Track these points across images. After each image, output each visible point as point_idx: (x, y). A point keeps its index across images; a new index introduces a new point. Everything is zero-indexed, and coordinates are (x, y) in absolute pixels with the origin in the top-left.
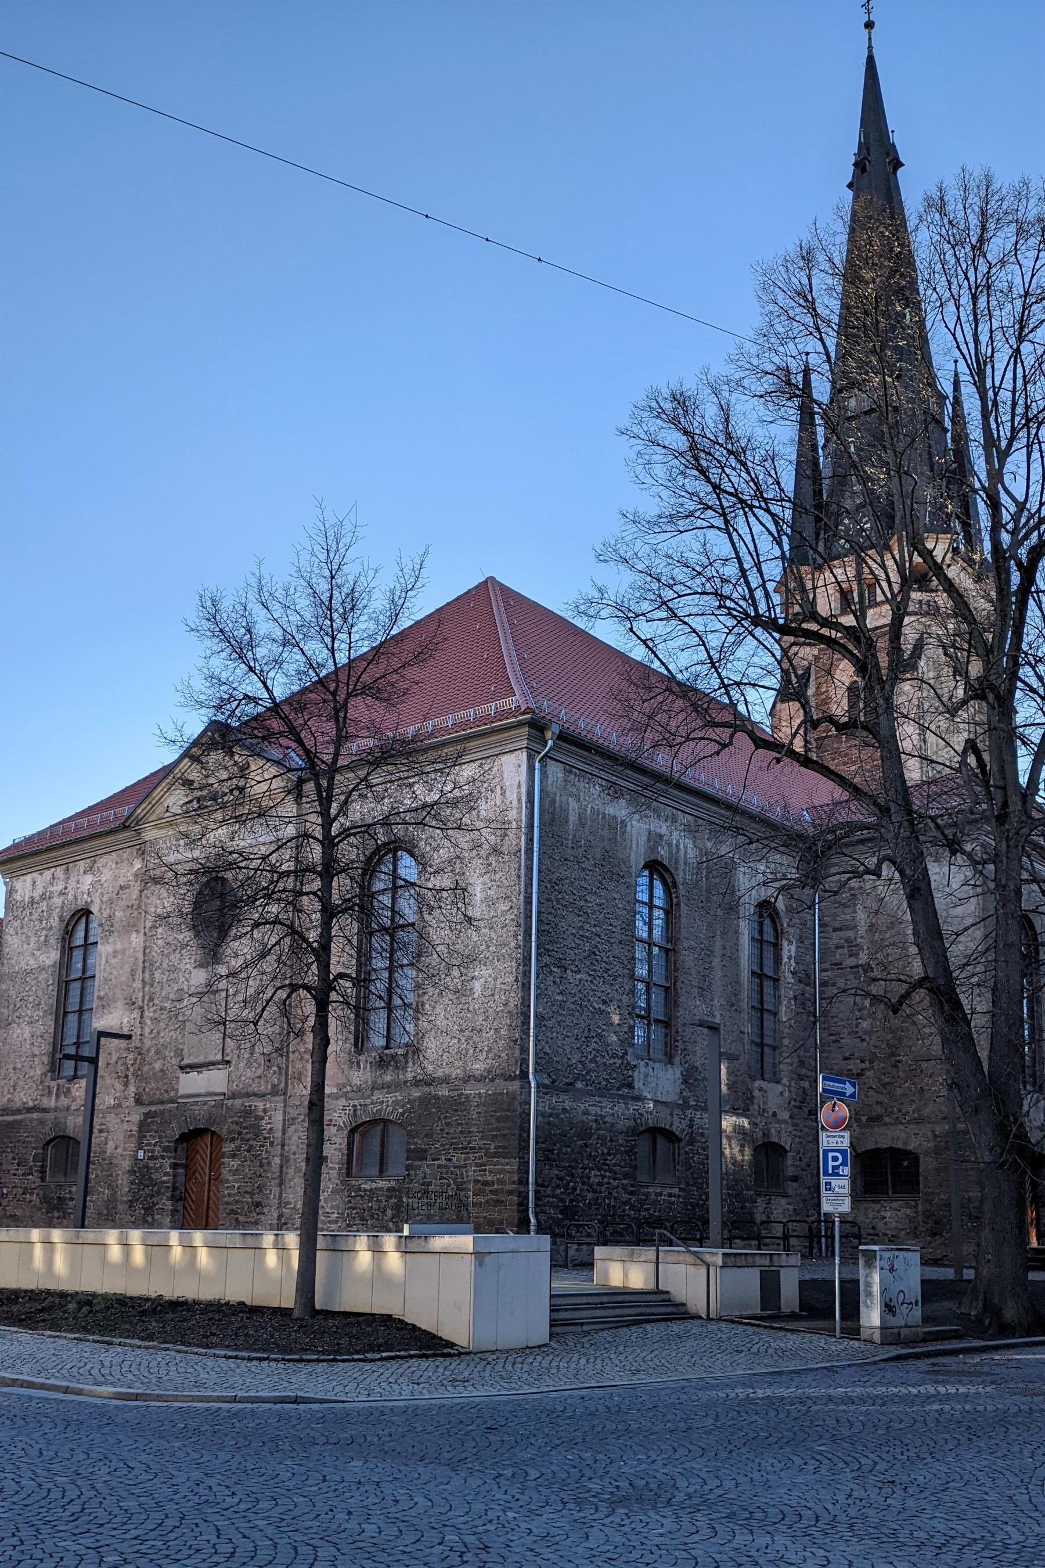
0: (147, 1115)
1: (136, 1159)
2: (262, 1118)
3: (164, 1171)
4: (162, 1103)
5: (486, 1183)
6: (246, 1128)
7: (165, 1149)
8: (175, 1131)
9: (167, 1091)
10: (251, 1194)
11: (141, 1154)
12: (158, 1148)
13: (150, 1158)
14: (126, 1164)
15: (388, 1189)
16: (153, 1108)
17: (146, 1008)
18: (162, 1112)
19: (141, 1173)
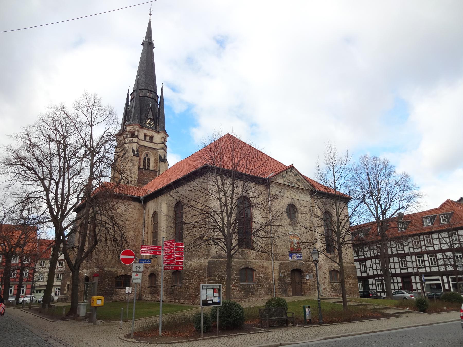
0: (281, 264)
1: (279, 276)
2: (313, 268)
3: (288, 279)
4: (284, 261)
5: (354, 283)
6: (309, 269)
7: (288, 274)
8: (290, 269)
10: (313, 286)
11: (281, 275)
12: (285, 273)
13: (283, 276)
14: (277, 278)
15: (338, 285)
16: (283, 262)
18: (286, 263)
19: (281, 280)
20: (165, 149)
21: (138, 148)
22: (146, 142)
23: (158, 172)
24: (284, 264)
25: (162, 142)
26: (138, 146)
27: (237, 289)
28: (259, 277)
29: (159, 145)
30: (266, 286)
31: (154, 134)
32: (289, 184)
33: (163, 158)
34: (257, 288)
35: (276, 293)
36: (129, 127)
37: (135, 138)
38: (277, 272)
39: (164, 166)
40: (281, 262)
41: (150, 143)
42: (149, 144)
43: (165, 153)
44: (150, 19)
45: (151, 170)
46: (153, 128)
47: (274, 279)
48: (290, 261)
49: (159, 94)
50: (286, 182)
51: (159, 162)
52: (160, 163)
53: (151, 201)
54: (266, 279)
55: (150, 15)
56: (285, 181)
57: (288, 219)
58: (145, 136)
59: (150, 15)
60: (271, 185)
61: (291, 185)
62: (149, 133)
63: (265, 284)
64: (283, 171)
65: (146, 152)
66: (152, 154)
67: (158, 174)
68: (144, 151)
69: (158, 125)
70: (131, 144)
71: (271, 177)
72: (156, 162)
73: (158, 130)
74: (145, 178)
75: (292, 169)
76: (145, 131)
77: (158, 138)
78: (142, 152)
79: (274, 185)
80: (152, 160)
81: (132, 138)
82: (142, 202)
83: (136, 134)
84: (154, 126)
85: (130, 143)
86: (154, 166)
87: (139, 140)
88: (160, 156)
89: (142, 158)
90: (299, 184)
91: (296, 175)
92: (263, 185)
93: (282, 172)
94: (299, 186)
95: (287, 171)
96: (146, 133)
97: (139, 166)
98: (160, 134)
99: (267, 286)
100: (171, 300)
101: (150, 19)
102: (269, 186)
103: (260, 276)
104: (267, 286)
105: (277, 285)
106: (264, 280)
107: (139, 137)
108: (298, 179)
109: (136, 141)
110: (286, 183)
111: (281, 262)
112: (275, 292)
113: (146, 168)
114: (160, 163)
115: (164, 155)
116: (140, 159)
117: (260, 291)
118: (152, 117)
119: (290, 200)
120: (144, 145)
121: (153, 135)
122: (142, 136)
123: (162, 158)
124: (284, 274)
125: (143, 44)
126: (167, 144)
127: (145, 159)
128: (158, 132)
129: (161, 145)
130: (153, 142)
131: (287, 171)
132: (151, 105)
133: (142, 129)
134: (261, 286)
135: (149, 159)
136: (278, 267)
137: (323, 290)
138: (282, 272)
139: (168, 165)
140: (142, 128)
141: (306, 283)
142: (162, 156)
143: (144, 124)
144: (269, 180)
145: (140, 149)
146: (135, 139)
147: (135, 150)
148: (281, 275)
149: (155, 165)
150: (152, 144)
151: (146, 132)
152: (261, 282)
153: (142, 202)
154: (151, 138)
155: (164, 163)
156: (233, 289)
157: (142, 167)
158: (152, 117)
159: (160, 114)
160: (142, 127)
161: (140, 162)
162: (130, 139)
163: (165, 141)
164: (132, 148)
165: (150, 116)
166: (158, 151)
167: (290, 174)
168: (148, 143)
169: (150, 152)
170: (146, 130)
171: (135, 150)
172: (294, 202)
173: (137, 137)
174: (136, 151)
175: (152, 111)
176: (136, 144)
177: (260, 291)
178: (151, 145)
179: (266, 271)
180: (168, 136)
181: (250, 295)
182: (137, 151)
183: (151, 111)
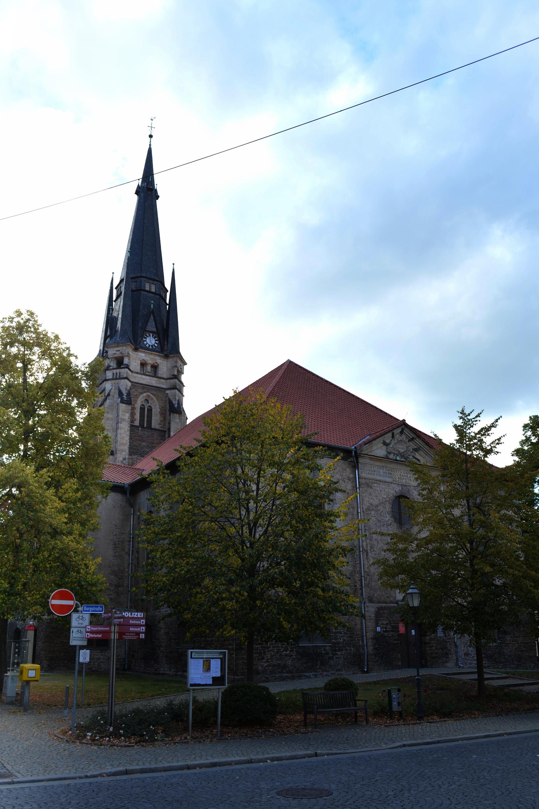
0: (379, 609)
4: (386, 603)
9: (388, 597)
11: (379, 629)
12: (389, 626)
13: (384, 631)
14: (370, 635)
16: (384, 605)
17: (369, 551)
20: (178, 387)
21: (128, 388)
22: (144, 377)
23: (167, 433)
24: (385, 608)
25: (174, 375)
26: (129, 384)
27: (291, 656)
28: (336, 633)
29: (168, 381)
30: (351, 650)
31: (159, 360)
32: (398, 458)
33: (176, 406)
34: (332, 654)
35: (369, 663)
36: (112, 349)
37: (123, 370)
38: (371, 624)
39: (178, 420)
40: (380, 605)
41: (151, 378)
42: (149, 380)
43: (179, 397)
44: (150, 145)
45: (155, 429)
46: (157, 349)
47: (365, 637)
48: (397, 603)
49: (168, 285)
50: (392, 455)
51: (168, 413)
52: (171, 416)
53: (143, 492)
54: (350, 637)
55: (151, 136)
56: (389, 453)
57: (395, 525)
58: (143, 365)
59: (151, 136)
60: (361, 460)
61: (402, 459)
62: (150, 358)
63: (348, 646)
64: (386, 433)
65: (145, 394)
66: (155, 399)
67: (167, 436)
68: (140, 393)
69: (166, 343)
70: (117, 381)
71: (360, 445)
72: (163, 413)
73: (165, 353)
74: (144, 444)
75: (403, 429)
76: (142, 355)
77: (164, 367)
78: (137, 396)
79: (367, 461)
80: (156, 410)
81: (118, 371)
82: (128, 492)
83: (126, 361)
84: (159, 346)
85: (116, 379)
86: (159, 421)
87: (130, 373)
88: (170, 402)
89: (138, 405)
90: (417, 456)
91: (412, 440)
92: (345, 462)
93: (382, 435)
94: (418, 460)
95: (393, 434)
96: (144, 360)
97: (132, 421)
98: (170, 360)
99: (352, 649)
100: (177, 672)
101: (150, 145)
102: (358, 462)
103: (338, 632)
104: (352, 649)
105: (372, 648)
106: (345, 638)
107: (131, 368)
108: (415, 447)
109: (125, 376)
110: (391, 456)
111: (380, 605)
112: (368, 661)
113: (145, 425)
114: (170, 415)
116: (133, 409)
117: (337, 658)
118: (155, 330)
119: (400, 488)
121: (156, 363)
122: (135, 365)
123: (173, 405)
124: (386, 628)
125: (137, 193)
126: (184, 378)
127: (142, 409)
128: (166, 357)
129: (172, 380)
130: (160, 376)
131: (393, 434)
132: (152, 307)
133: (137, 353)
134: (339, 651)
135: (150, 410)
136: (373, 616)
137: (463, 656)
138: (382, 624)
139: (187, 419)
140: (136, 349)
141: (430, 643)
142: (175, 403)
143: (140, 342)
144: (356, 452)
145: (133, 390)
146: (124, 372)
147: (124, 392)
148: (379, 629)
149: (162, 419)
151: (144, 358)
152: (339, 643)
153: (128, 492)
154: (155, 367)
155: (178, 415)
156: (286, 655)
157: (137, 423)
158: (155, 330)
159: (170, 322)
160: (138, 346)
161: (132, 415)
162: (115, 371)
163: (181, 372)
164: (119, 387)
165: (151, 326)
166: (167, 392)
167: (400, 438)
168: (148, 377)
169: (151, 395)
170: (143, 355)
171: (124, 392)
172: (408, 492)
173: (127, 367)
174: (126, 395)
175: (154, 317)
176: (126, 380)
177: (337, 658)
178: (153, 381)
179: (349, 622)
180: (185, 363)
181: (318, 667)
182: (129, 394)
183: (152, 317)
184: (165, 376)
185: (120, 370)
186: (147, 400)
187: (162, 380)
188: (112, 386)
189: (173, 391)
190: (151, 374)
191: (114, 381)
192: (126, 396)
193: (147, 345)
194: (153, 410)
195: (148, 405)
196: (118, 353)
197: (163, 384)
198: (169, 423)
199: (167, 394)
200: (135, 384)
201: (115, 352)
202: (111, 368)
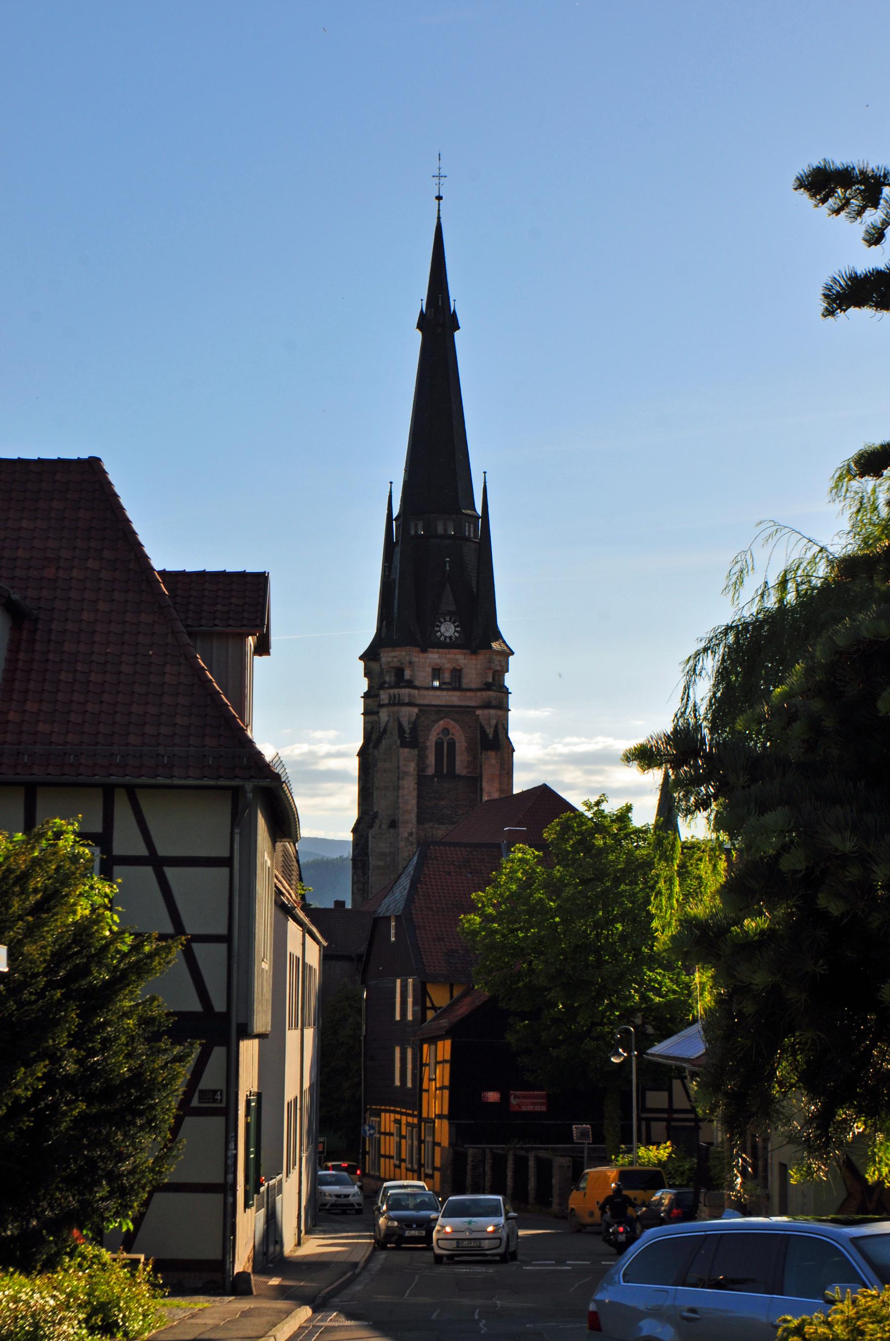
29: (479, 694)
33: (491, 736)
41: (450, 693)
58: (437, 672)
70: (396, 709)
81: (396, 691)
83: (407, 674)
107: (417, 683)
109: (407, 700)
113: (445, 771)
115: (496, 726)
120: (434, 703)
126: (509, 680)
150: (458, 693)
154: (457, 673)
162: (392, 691)
164: (398, 719)
166: (478, 712)
168: (445, 693)
174: (408, 732)
178: (454, 698)
184: (473, 686)
185: (400, 690)
186: (446, 731)
187: (469, 694)
188: (389, 716)
189: (486, 712)
190: (450, 687)
191: (392, 709)
192: (410, 734)
193: (442, 638)
194: (457, 745)
195: (448, 738)
196: (395, 660)
197: (471, 699)
198: (481, 767)
199: (478, 715)
200: (424, 709)
201: (390, 659)
202: (387, 685)
